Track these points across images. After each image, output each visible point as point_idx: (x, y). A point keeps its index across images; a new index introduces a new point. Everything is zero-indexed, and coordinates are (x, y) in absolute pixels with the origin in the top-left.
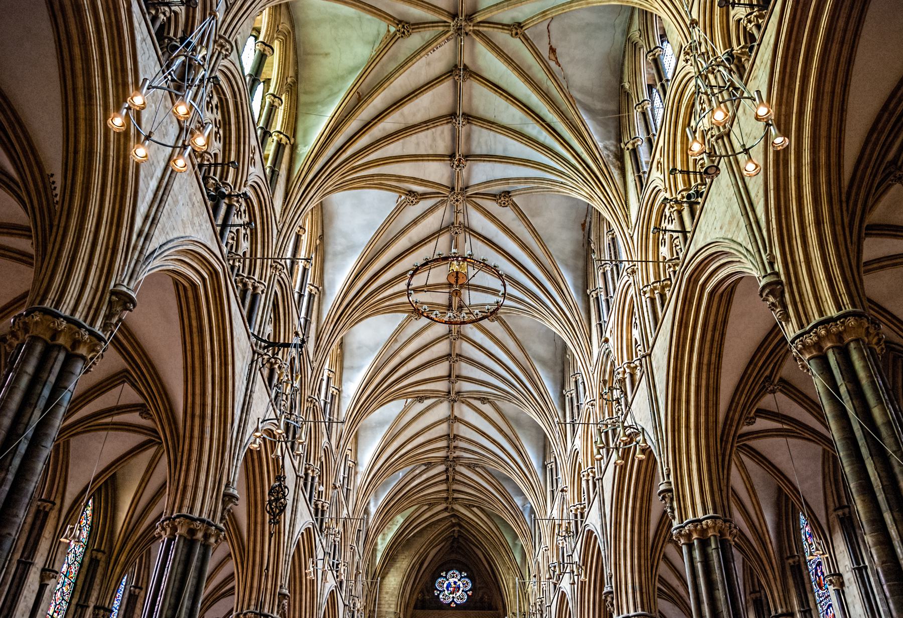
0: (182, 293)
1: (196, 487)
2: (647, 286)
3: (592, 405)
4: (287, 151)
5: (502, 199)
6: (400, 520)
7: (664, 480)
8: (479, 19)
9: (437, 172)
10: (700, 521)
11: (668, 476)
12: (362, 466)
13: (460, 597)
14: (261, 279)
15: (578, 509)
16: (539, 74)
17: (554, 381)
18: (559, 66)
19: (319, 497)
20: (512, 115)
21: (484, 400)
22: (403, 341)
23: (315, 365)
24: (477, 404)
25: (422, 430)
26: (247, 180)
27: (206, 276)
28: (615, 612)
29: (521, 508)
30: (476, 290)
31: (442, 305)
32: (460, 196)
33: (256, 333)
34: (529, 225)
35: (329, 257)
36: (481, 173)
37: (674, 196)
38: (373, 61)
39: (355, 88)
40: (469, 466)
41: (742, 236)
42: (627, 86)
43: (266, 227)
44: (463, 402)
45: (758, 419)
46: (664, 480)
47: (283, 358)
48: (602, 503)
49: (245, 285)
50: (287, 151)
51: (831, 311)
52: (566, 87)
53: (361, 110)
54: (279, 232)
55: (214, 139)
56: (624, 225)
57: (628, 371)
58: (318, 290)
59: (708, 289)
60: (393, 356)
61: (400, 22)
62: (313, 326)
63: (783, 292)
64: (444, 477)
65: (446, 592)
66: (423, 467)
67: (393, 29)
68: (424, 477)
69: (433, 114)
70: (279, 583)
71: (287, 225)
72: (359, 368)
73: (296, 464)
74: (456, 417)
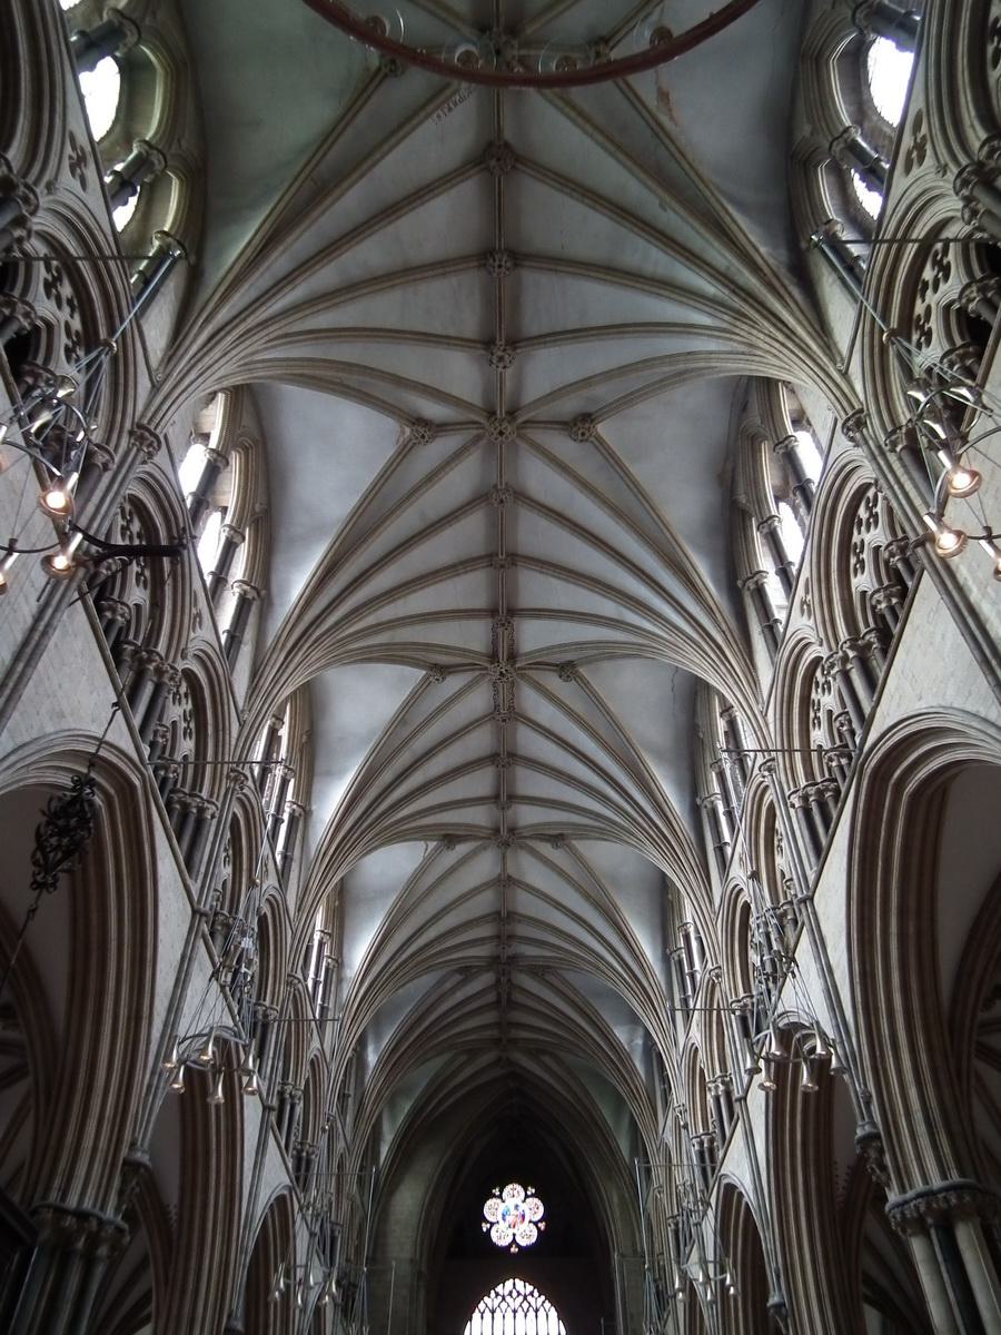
3: (769, 770)
5: (580, 425)
12: (351, 968)
13: (527, 1236)
17: (679, 784)
19: (258, 998)
21: (558, 839)
22: (418, 723)
23: (249, 717)
24: (545, 849)
25: (454, 902)
28: (894, 1183)
29: (626, 1047)
32: (505, 424)
44: (521, 848)
48: (820, 944)
57: (851, 654)
58: (258, 593)
64: (491, 997)
65: (502, 1226)
66: (458, 977)
68: (459, 996)
70: (127, 1137)
72: (341, 773)
73: (195, 888)
74: (509, 877)
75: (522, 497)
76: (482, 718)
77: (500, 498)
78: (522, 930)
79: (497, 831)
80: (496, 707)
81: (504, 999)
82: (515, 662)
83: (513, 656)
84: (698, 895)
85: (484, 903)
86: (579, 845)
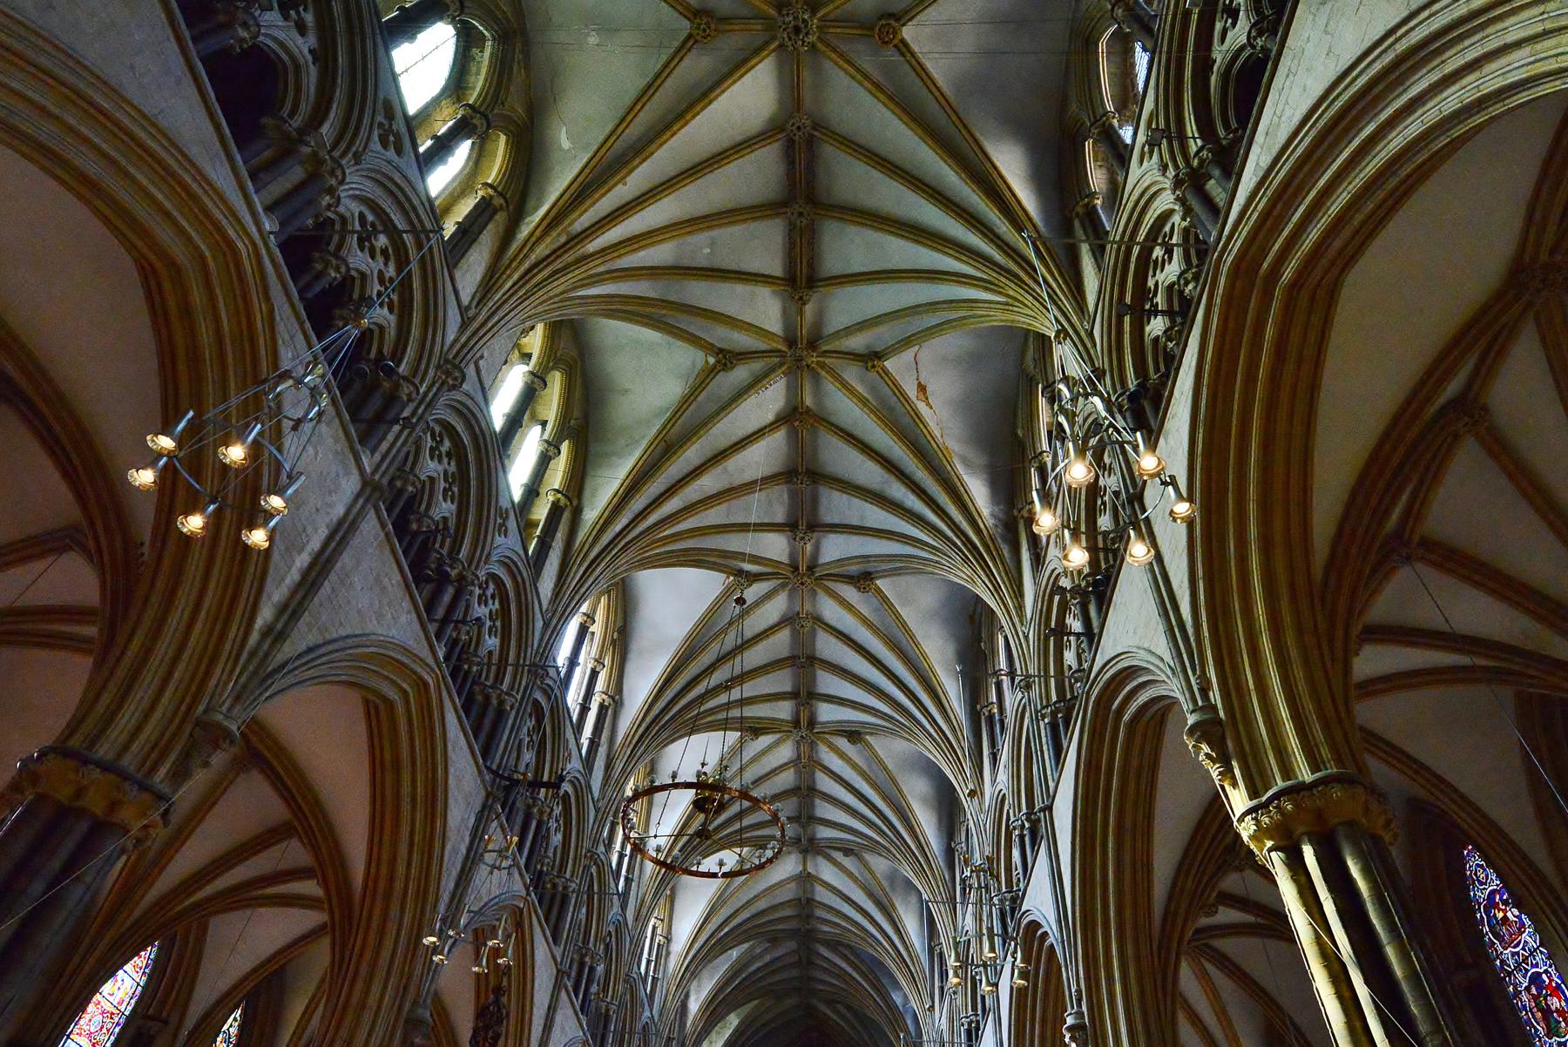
0: (372, 712)
2: (1047, 707)
4: (566, 516)
6: (733, 1021)
7: (1072, 1008)
8: (825, 348)
9: (776, 546)
11: (1079, 1001)
14: (512, 689)
15: (972, 1022)
18: (931, 408)
20: (869, 473)
21: (848, 852)
24: (838, 856)
26: (489, 554)
27: (408, 689)
29: (901, 1008)
30: (832, 702)
31: (787, 721)
32: (805, 579)
33: (494, 767)
36: (834, 548)
37: (1077, 582)
39: (661, 436)
41: (1162, 647)
42: (1020, 432)
43: (524, 618)
44: (819, 854)
45: (1221, 908)
46: (1072, 1008)
47: (546, 799)
49: (487, 698)
50: (566, 516)
52: (939, 436)
53: (668, 463)
54: (546, 625)
55: (441, 498)
56: (1016, 620)
57: (1027, 825)
58: (614, 700)
59: (1126, 717)
61: (721, 351)
62: (602, 751)
63: (1223, 738)
67: (712, 360)
68: (768, 958)
71: (558, 615)
75: (818, 620)
76: (786, 764)
77: (800, 623)
78: (820, 913)
79: (799, 840)
80: (799, 755)
81: (806, 961)
82: (813, 729)
83: (812, 723)
84: (946, 920)
85: (787, 894)
86: (868, 857)
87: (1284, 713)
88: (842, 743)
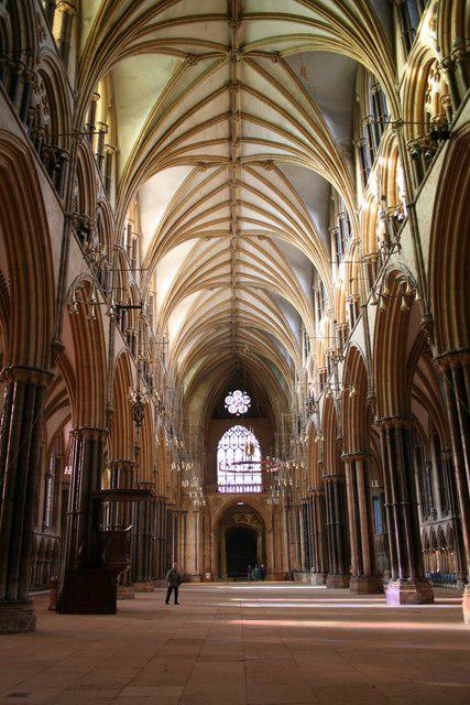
1: (90, 410)
6: (199, 364)
9: (220, 150)
10: (390, 419)
13: (243, 409)
16: (293, 87)
17: (306, 279)
21: (256, 288)
23: (141, 291)
34: (287, 181)
35: (143, 209)
36: (251, 149)
38: (172, 83)
40: (247, 328)
50: (114, 157)
51: (457, 347)
54: (116, 223)
60: (192, 266)
61: (189, 54)
69: (216, 114)
83: (239, 231)
87: (455, 322)
88: (256, 240)
